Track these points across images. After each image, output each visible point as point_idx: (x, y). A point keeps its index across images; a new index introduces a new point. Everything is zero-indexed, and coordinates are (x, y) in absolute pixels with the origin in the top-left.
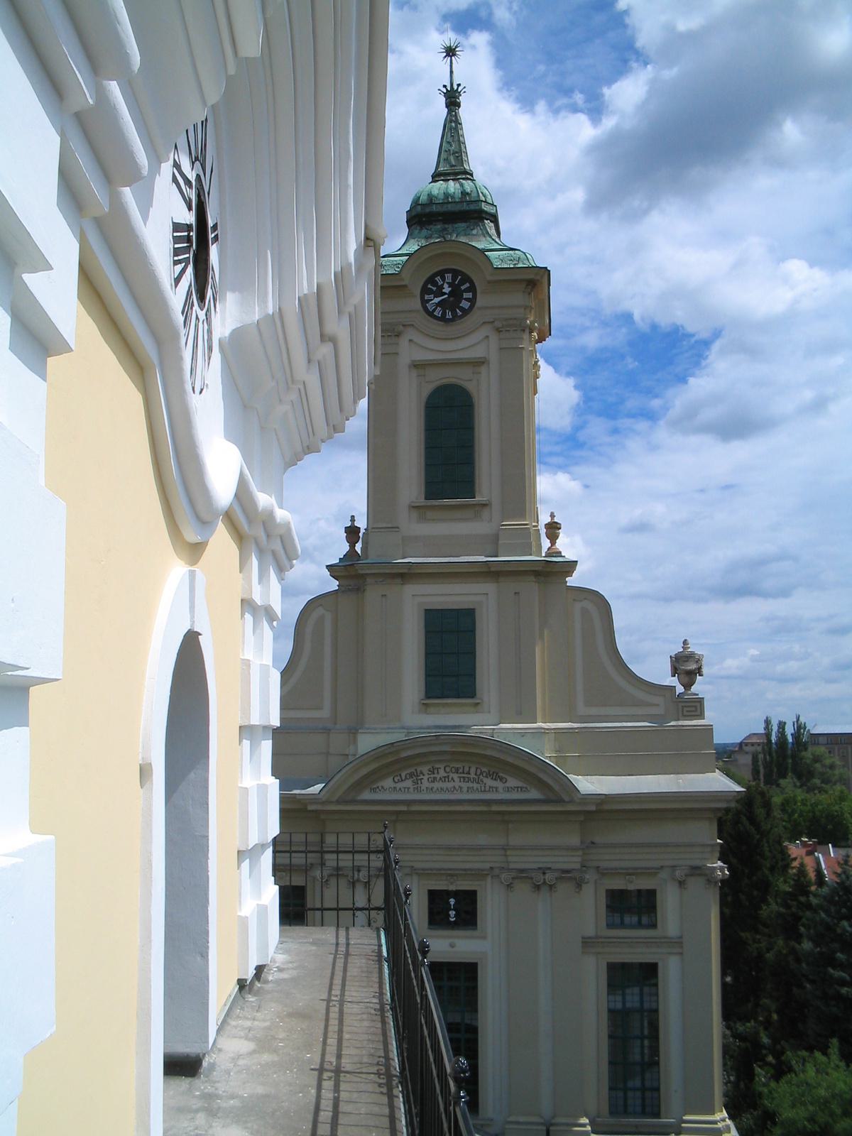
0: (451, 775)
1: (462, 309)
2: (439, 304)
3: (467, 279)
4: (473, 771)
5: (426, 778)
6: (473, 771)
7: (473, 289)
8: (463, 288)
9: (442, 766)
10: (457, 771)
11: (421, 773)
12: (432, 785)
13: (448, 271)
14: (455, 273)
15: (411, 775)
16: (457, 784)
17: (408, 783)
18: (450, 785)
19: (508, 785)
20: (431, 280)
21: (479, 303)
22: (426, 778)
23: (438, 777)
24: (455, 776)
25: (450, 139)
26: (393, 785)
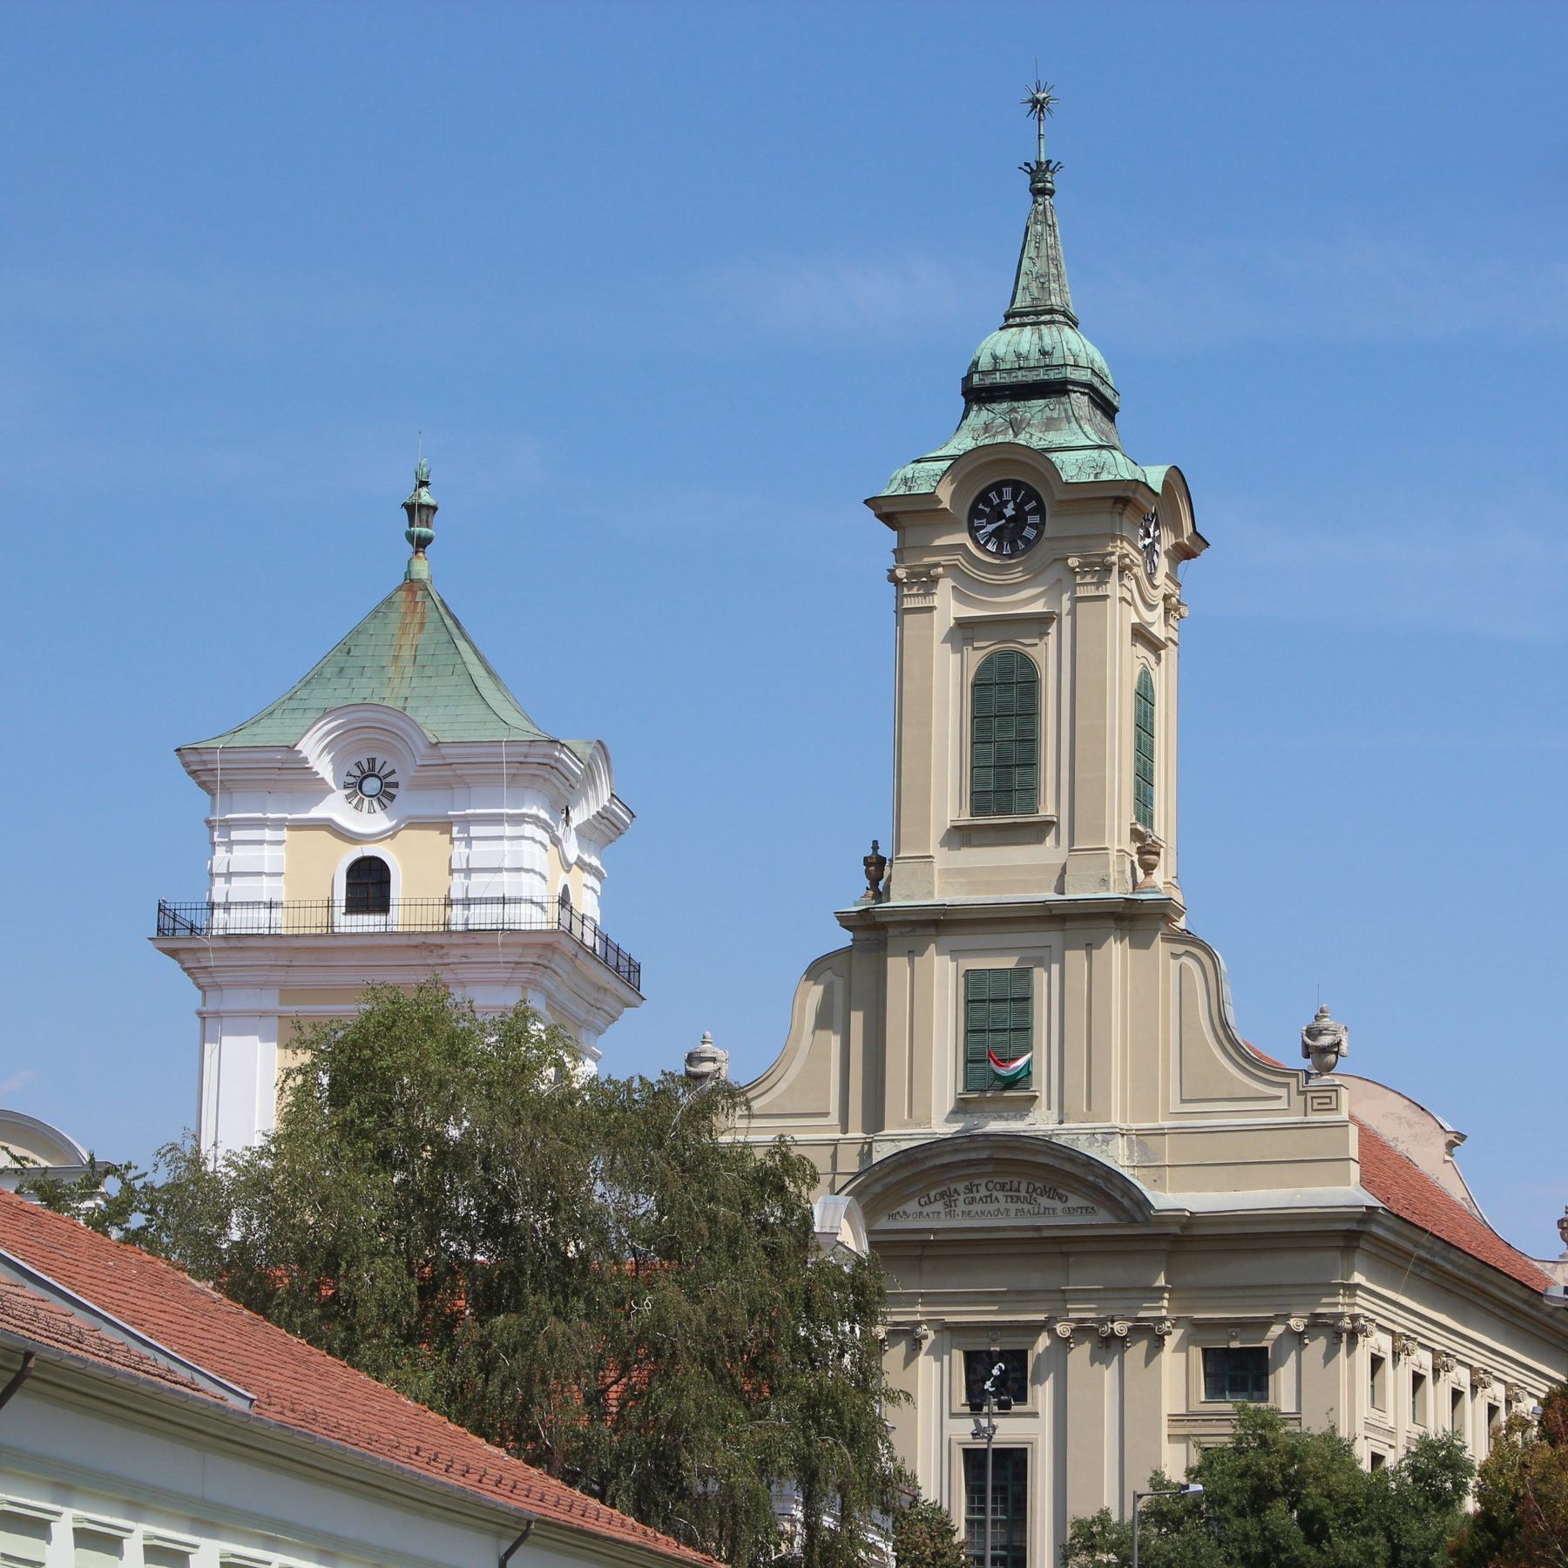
0: (995, 1194)
1: (1027, 541)
2: (992, 534)
3: (1033, 495)
4: (1023, 1186)
5: (961, 1198)
6: (1023, 1186)
7: (1040, 510)
8: (1027, 508)
9: (983, 1182)
10: (1003, 1188)
11: (956, 1191)
12: (970, 1207)
13: (1006, 483)
14: (1017, 486)
15: (942, 1195)
16: (1002, 1205)
17: (939, 1206)
18: (992, 1207)
19: (1069, 1204)
20: (983, 497)
21: (1049, 530)
22: (961, 1198)
23: (978, 1196)
24: (1000, 1195)
25: (1033, 254)
26: (920, 1209)
